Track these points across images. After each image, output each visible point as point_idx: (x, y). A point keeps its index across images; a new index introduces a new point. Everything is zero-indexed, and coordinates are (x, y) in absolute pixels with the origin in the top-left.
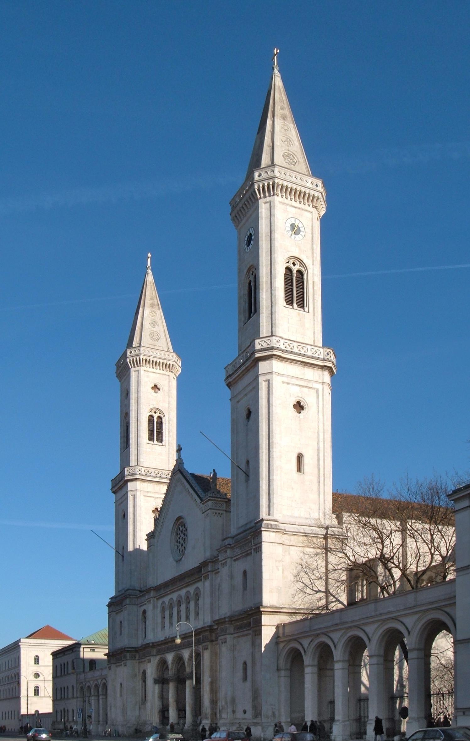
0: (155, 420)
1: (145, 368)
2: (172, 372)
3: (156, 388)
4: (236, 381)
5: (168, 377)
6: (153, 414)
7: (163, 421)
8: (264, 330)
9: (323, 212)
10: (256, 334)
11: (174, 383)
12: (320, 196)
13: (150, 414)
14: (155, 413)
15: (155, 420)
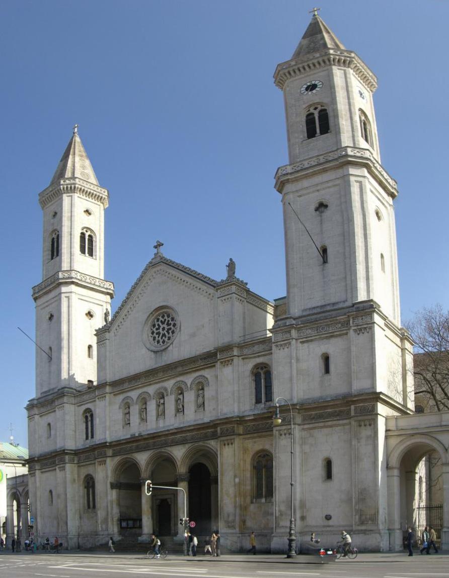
0: (87, 238)
1: (78, 195)
2: (103, 203)
3: (87, 212)
4: (40, 297)
5: (99, 206)
6: (85, 232)
7: (94, 239)
8: (65, 266)
9: (107, 206)
10: (59, 269)
11: (103, 212)
12: (106, 197)
13: (82, 231)
14: (87, 231)
15: (87, 238)
